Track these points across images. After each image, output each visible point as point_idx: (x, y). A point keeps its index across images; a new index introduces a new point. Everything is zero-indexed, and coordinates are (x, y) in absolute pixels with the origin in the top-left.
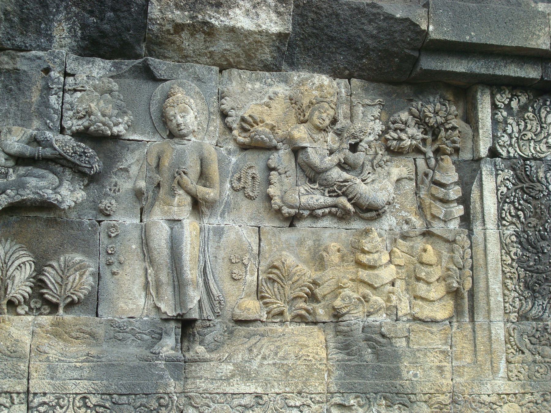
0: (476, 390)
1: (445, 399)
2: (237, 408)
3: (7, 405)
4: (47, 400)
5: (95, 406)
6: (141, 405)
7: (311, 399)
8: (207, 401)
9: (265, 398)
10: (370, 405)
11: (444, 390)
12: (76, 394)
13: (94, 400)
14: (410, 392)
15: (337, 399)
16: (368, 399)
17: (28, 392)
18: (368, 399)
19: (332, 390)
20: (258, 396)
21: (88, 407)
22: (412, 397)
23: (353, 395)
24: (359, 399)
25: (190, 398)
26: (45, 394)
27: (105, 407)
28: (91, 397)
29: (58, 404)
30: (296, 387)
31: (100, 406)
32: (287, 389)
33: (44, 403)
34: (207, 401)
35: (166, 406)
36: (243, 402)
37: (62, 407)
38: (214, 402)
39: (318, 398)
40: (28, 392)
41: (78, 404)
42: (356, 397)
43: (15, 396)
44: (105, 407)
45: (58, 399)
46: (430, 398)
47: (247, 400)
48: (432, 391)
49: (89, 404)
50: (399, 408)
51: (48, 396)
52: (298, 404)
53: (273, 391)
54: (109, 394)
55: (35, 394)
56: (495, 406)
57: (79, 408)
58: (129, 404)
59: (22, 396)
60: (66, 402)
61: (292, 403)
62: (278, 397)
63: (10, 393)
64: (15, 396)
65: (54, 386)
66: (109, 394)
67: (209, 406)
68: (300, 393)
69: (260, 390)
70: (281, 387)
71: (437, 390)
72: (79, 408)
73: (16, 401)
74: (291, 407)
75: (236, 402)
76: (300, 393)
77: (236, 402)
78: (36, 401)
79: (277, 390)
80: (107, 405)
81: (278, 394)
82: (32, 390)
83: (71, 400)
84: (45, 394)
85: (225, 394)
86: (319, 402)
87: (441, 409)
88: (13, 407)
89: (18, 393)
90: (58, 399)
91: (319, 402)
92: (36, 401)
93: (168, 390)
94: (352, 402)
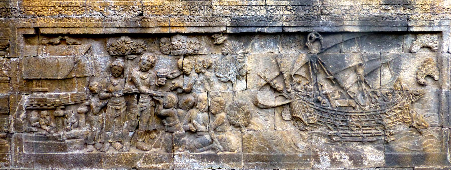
0: (442, 3)
1: (428, 7)
2: (344, 10)
3: (259, 10)
4: (273, 8)
5: (290, 10)
6: (307, 9)
7: (373, 7)
8: (332, 8)
9: (354, 6)
10: (397, 9)
11: (428, 3)
12: (283, 5)
13: (290, 8)
14: (413, 4)
15: (383, 7)
16: (396, 6)
17: (266, 5)
18: (396, 6)
19: (381, 3)
20: (351, 6)
21: (288, 10)
22: (414, 6)
23: (390, 5)
24: (392, 7)
25: (325, 7)
26: (272, 6)
27: (294, 10)
28: (289, 6)
29: (277, 9)
30: (367, 2)
31: (292, 10)
32: (363, 3)
33: (272, 9)
34: (332, 8)
35: (316, 10)
36: (346, 8)
37: (278, 10)
38: (334, 8)
39: (375, 6)
40: (266, 5)
41: (284, 9)
42: (391, 6)
43: (261, 6)
44: (294, 10)
45: (277, 7)
46: (422, 6)
47: (347, 7)
48: (423, 4)
49: (288, 9)
50: (409, 10)
51: (273, 6)
52: (367, 9)
53: (357, 4)
54: (295, 5)
55: (268, 6)
56: (450, 10)
57: (285, 10)
58: (303, 9)
59: (264, 6)
60: (280, 8)
61: (365, 8)
62: (359, 6)
63: (259, 5)
64: (261, 6)
65: (275, 3)
66: (295, 5)
67: (333, 10)
68: (368, 5)
69: (352, 4)
70: (361, 2)
71: (425, 3)
72: (285, 10)
73: (262, 8)
74: (365, 10)
75: (343, 8)
76: (368, 5)
77: (343, 8)
78: (269, 8)
79: (359, 4)
80: (295, 9)
81: (359, 5)
82: (267, 4)
83: (281, 7)
84: (272, 6)
85: (338, 5)
86: (376, 8)
87: (426, 11)
88: (261, 10)
89: (262, 5)
90: (277, 7)
91: (376, 8)
92: (269, 8)
93: (317, 4)
94: (389, 8)
